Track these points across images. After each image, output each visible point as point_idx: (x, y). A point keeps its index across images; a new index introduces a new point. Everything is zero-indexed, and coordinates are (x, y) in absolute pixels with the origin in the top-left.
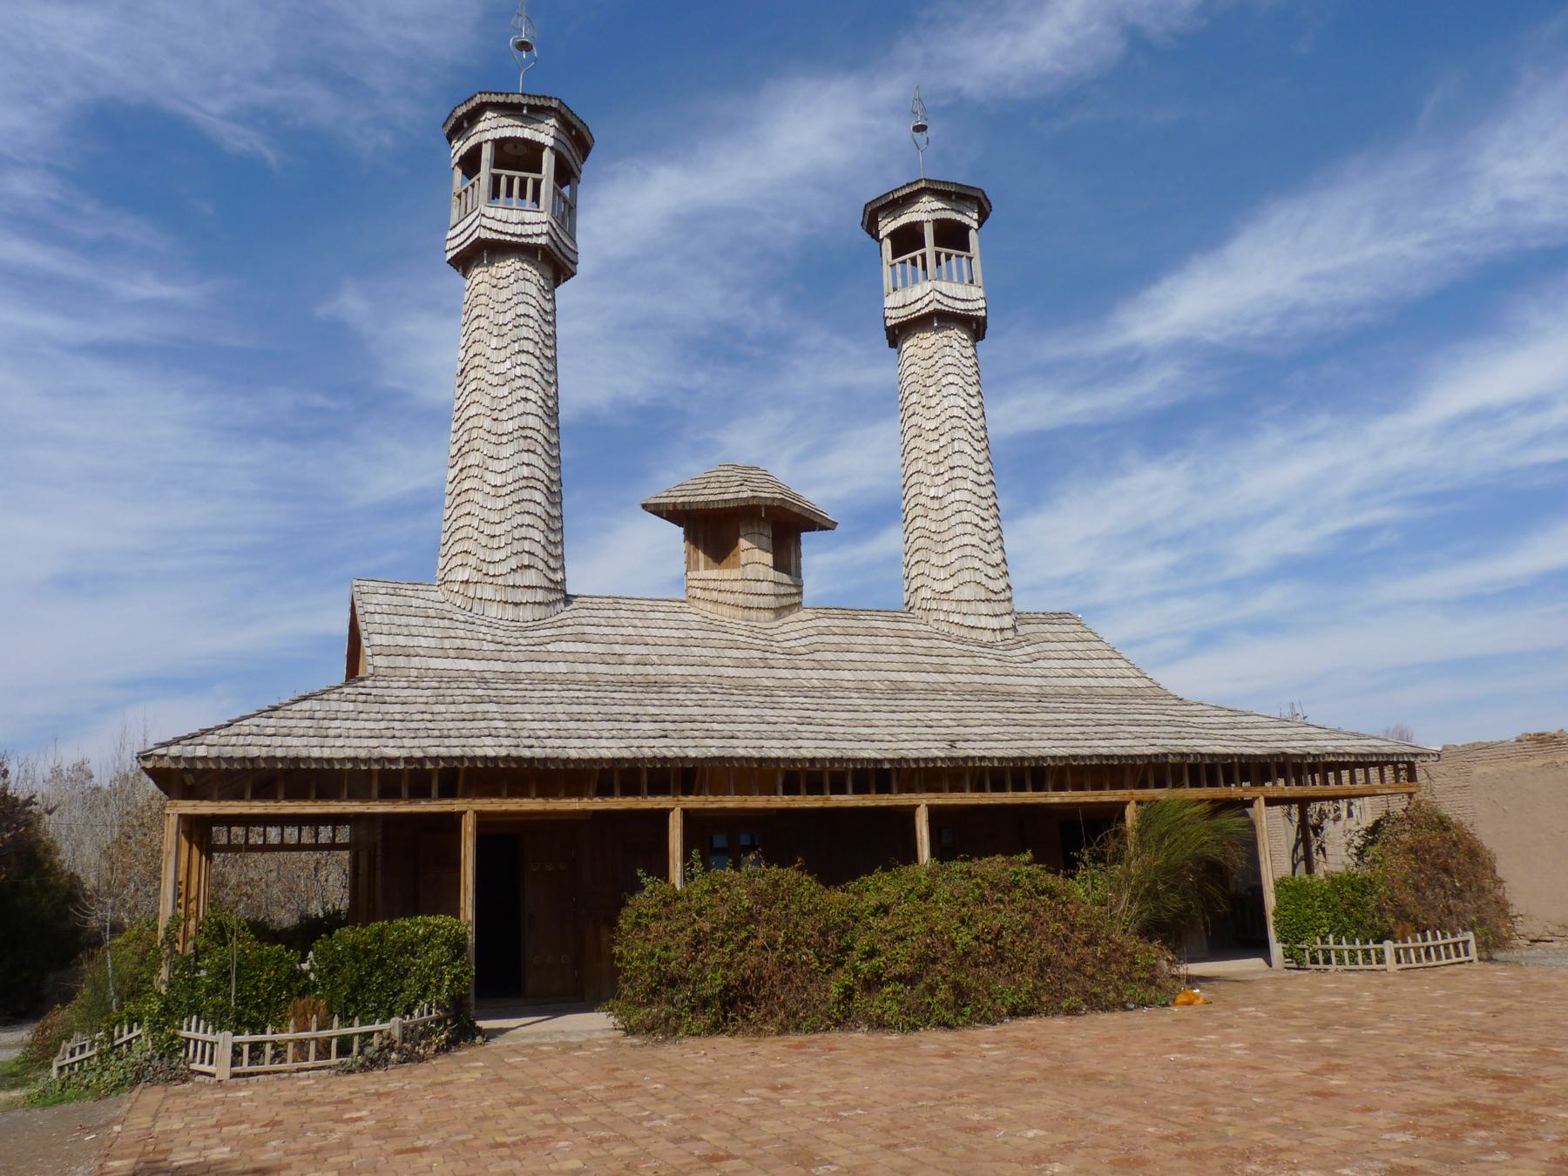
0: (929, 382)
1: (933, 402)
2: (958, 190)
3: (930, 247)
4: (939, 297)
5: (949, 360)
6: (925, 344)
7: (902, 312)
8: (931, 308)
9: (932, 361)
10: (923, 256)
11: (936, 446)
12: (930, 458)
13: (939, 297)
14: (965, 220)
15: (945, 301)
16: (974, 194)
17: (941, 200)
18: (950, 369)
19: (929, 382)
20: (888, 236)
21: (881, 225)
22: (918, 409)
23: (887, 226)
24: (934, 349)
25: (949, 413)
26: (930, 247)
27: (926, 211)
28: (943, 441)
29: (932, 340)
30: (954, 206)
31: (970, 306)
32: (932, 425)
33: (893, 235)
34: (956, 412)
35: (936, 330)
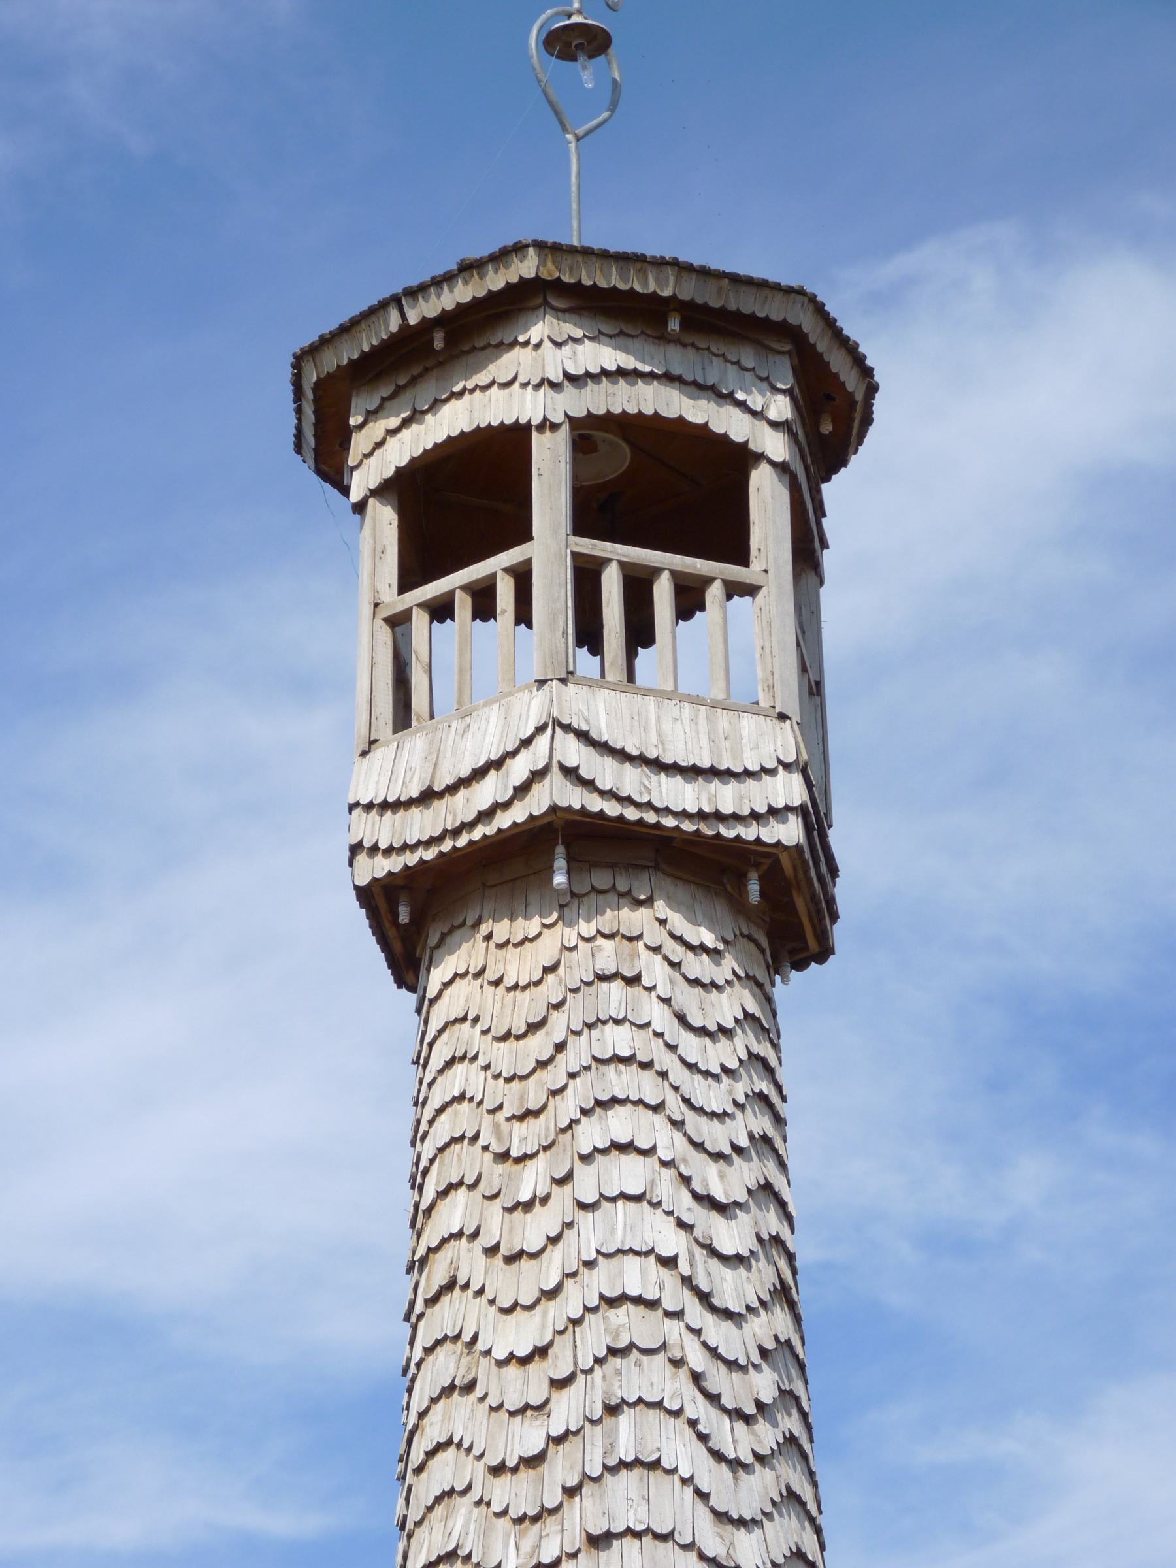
0: (522, 1138)
1: (533, 1230)
2: (688, 290)
3: (550, 540)
4: (573, 752)
5: (619, 1040)
6: (518, 966)
7: (420, 824)
8: (537, 803)
9: (539, 1045)
10: (522, 576)
11: (529, 1437)
12: (502, 1491)
13: (573, 752)
14: (731, 424)
15: (606, 772)
16: (775, 310)
17: (616, 338)
18: (620, 1081)
19: (522, 1138)
20: (382, 491)
21: (360, 443)
22: (469, 1261)
23: (388, 446)
24: (552, 989)
25: (601, 1282)
26: (550, 540)
27: (541, 382)
28: (567, 1410)
29: (547, 949)
30: (679, 361)
31: (727, 797)
32: (519, 1336)
33: (404, 487)
34: (637, 1277)
35: (568, 905)
